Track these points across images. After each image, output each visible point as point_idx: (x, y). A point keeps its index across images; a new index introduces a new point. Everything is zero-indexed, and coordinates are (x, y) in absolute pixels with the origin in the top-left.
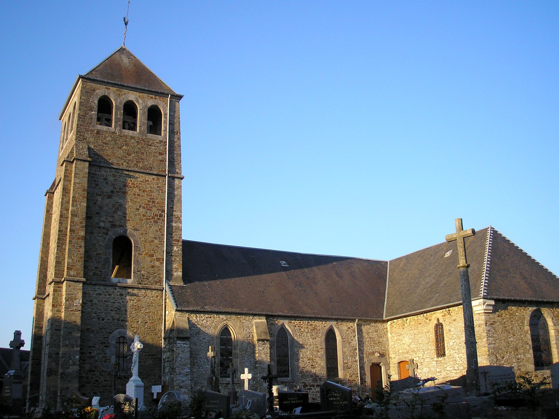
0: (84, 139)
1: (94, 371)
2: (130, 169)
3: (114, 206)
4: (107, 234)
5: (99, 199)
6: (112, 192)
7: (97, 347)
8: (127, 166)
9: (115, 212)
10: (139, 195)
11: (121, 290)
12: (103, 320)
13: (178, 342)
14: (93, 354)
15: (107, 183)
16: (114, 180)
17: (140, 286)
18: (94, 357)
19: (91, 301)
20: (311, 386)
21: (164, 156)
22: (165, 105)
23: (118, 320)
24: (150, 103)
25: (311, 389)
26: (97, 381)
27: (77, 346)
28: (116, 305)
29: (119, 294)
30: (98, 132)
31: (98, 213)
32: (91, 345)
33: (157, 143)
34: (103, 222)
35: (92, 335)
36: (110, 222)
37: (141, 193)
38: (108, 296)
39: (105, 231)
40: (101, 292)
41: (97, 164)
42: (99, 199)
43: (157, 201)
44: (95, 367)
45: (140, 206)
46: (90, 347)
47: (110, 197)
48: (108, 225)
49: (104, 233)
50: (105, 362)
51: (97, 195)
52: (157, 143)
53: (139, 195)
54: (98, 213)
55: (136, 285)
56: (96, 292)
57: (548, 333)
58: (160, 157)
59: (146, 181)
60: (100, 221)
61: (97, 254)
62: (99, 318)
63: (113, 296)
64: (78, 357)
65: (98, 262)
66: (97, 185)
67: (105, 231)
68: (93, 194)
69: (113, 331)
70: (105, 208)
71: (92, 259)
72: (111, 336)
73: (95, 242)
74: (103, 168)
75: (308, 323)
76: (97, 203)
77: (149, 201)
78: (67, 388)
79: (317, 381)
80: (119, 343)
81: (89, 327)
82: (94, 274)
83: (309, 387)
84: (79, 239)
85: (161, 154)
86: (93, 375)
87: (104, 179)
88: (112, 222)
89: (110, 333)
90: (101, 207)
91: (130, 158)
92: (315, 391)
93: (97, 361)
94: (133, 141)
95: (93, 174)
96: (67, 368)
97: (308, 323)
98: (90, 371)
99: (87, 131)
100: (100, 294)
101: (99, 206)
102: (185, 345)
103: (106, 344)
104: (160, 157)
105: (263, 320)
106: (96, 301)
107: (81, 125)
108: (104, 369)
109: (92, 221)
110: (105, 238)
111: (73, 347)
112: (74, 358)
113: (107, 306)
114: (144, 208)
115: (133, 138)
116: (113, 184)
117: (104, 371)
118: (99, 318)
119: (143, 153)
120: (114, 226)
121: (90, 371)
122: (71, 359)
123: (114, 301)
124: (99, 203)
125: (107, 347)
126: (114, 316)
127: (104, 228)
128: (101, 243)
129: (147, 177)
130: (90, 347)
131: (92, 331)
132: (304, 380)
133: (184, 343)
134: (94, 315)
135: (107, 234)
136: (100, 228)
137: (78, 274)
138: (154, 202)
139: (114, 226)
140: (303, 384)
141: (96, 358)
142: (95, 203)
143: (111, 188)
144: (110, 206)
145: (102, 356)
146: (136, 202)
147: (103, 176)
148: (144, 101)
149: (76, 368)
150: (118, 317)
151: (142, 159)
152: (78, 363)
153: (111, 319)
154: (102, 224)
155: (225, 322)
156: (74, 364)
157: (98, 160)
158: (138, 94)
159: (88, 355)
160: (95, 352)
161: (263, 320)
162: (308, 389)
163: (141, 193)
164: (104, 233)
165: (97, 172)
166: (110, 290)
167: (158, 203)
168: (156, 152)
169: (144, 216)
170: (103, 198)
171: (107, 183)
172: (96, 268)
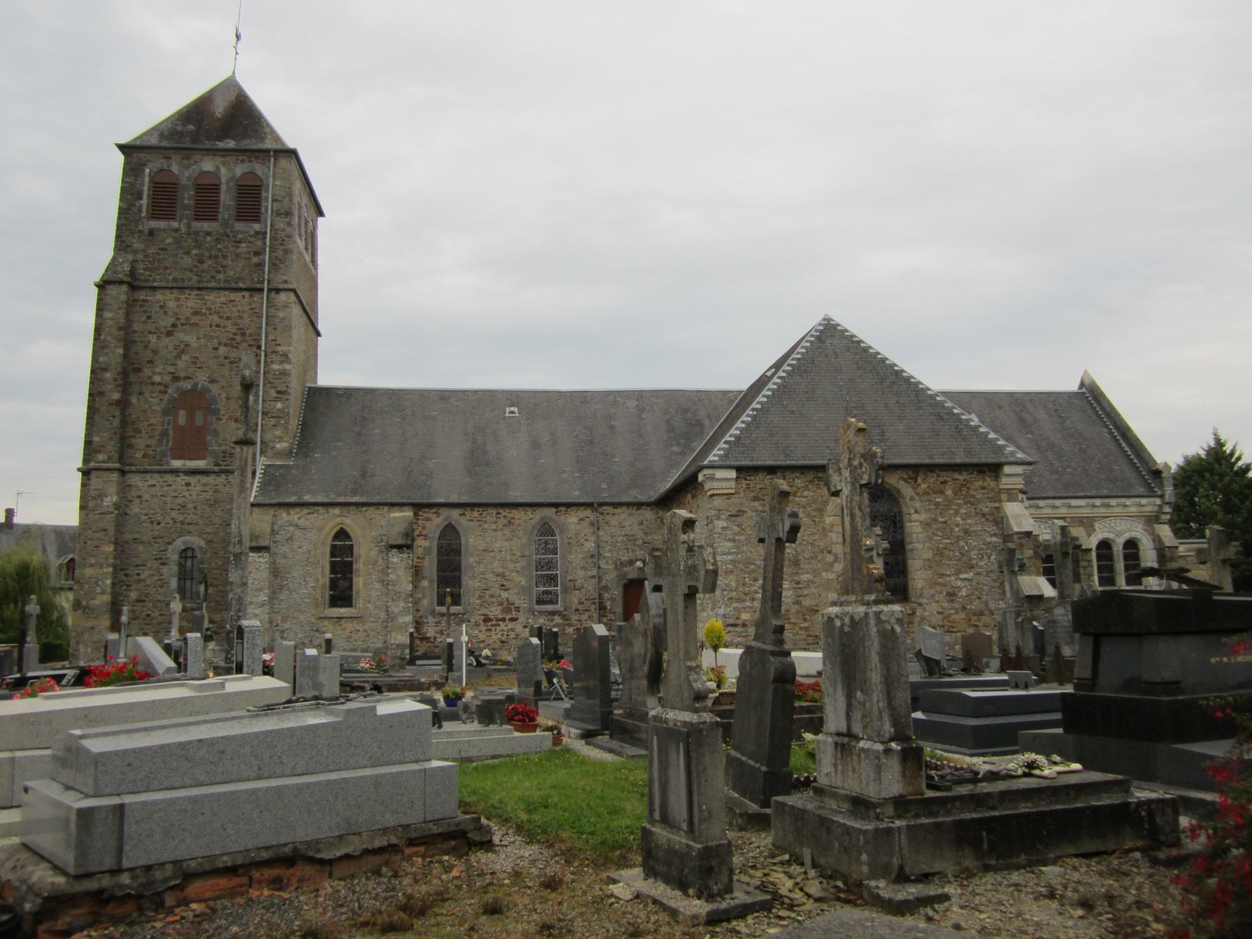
0: (127, 246)
1: (144, 601)
2: (201, 285)
3: (176, 347)
4: (165, 392)
5: (153, 338)
6: (174, 325)
7: (149, 565)
8: (199, 282)
9: (178, 357)
10: (218, 326)
11: (187, 478)
12: (159, 524)
13: (251, 554)
14: (142, 577)
15: (165, 313)
16: (178, 306)
17: (216, 469)
18: (144, 580)
19: (140, 497)
20: (498, 620)
21: (262, 257)
22: (266, 169)
23: (182, 523)
24: (239, 170)
25: (499, 625)
26: (149, 615)
27: (108, 566)
28: (180, 500)
29: (183, 483)
30: (151, 233)
31: (150, 362)
32: (140, 562)
33: (251, 236)
34: (159, 374)
35: (141, 548)
36: (170, 373)
37: (222, 322)
38: (166, 488)
39: (161, 388)
40: (154, 482)
41: (148, 284)
42: (153, 338)
43: (248, 332)
44: (147, 595)
45: (220, 344)
46: (138, 565)
47: (169, 334)
48: (167, 378)
49: (160, 392)
50: (161, 587)
51: (150, 333)
52: (251, 236)
53: (218, 326)
54: (150, 362)
55: (211, 467)
56: (147, 484)
57: (902, 528)
58: (255, 260)
59: (231, 301)
60: (154, 373)
61: (149, 425)
62: (152, 522)
63: (174, 487)
64: (109, 582)
65: (150, 437)
66: (149, 318)
67: (161, 388)
68: (142, 333)
69: (174, 541)
70: (163, 352)
71: (141, 432)
72: (170, 548)
73: (146, 406)
74: (160, 291)
75: (498, 513)
76: (150, 345)
77: (235, 334)
78: (93, 628)
79: (510, 611)
80: (186, 557)
81: (136, 536)
82: (145, 456)
83: (494, 622)
84: (111, 404)
85: (257, 254)
86: (143, 607)
87: (161, 307)
88: (173, 373)
89: (169, 543)
90: (155, 352)
91: (205, 266)
92: (505, 628)
93: (149, 586)
94: (209, 238)
95: (143, 300)
96: (94, 599)
97: (498, 513)
98: (138, 601)
99: (133, 233)
100: (154, 486)
101: (153, 351)
102: (261, 559)
103: (163, 561)
104: (255, 260)
105: (407, 514)
106: (146, 496)
107: (124, 225)
108: (159, 598)
109: (141, 374)
110: (161, 400)
111: (101, 567)
112: (103, 583)
113: (165, 503)
114: (226, 345)
115: (208, 233)
116: (176, 314)
117: (159, 601)
118: (152, 522)
119: (225, 257)
120: (176, 379)
121: (138, 601)
122: (98, 585)
123: (176, 494)
124: (152, 346)
125: (164, 564)
126: (176, 517)
127: (160, 384)
128: (155, 408)
129: (233, 296)
130: (138, 565)
131: (142, 542)
132: (485, 611)
133: (260, 557)
134: (144, 518)
135: (165, 392)
136: (153, 384)
137: (109, 459)
138: (243, 334)
139: (176, 379)
140: (483, 617)
141: (148, 582)
142: (146, 347)
143: (172, 320)
144: (171, 348)
145: (156, 578)
146: (212, 337)
147: (160, 302)
148: (229, 169)
149: (107, 598)
150: (181, 518)
151: (223, 267)
152: (109, 590)
153: (171, 522)
154: (157, 379)
155: (338, 520)
156: (103, 593)
157: (151, 278)
158: (219, 159)
159: (136, 577)
160: (147, 573)
161: (407, 514)
162: (492, 625)
163: (222, 322)
164: (160, 392)
165: (149, 298)
166: (170, 478)
167: (250, 335)
168: (249, 253)
169: (226, 358)
170: (159, 338)
171: (165, 313)
172: (148, 446)
